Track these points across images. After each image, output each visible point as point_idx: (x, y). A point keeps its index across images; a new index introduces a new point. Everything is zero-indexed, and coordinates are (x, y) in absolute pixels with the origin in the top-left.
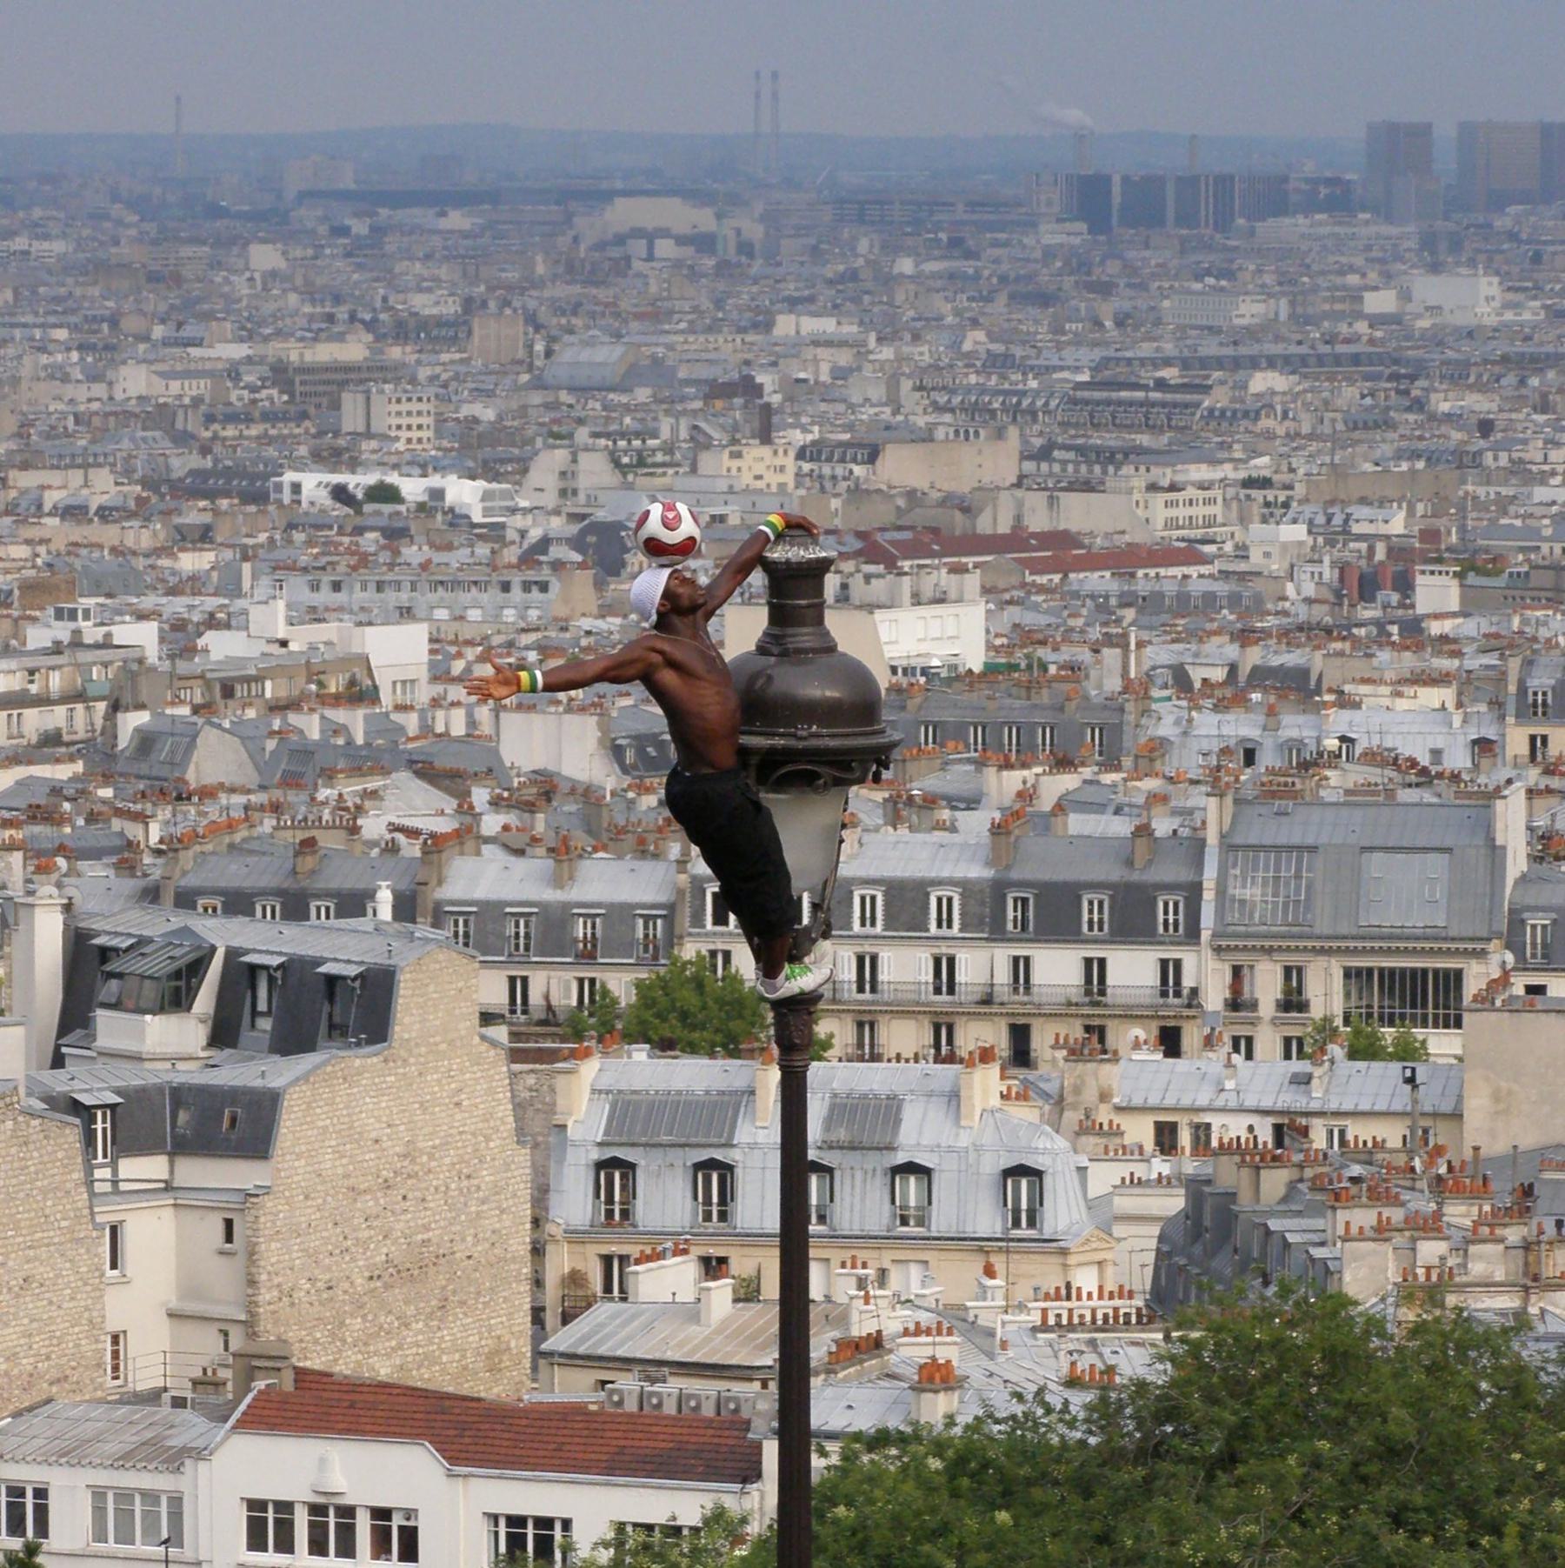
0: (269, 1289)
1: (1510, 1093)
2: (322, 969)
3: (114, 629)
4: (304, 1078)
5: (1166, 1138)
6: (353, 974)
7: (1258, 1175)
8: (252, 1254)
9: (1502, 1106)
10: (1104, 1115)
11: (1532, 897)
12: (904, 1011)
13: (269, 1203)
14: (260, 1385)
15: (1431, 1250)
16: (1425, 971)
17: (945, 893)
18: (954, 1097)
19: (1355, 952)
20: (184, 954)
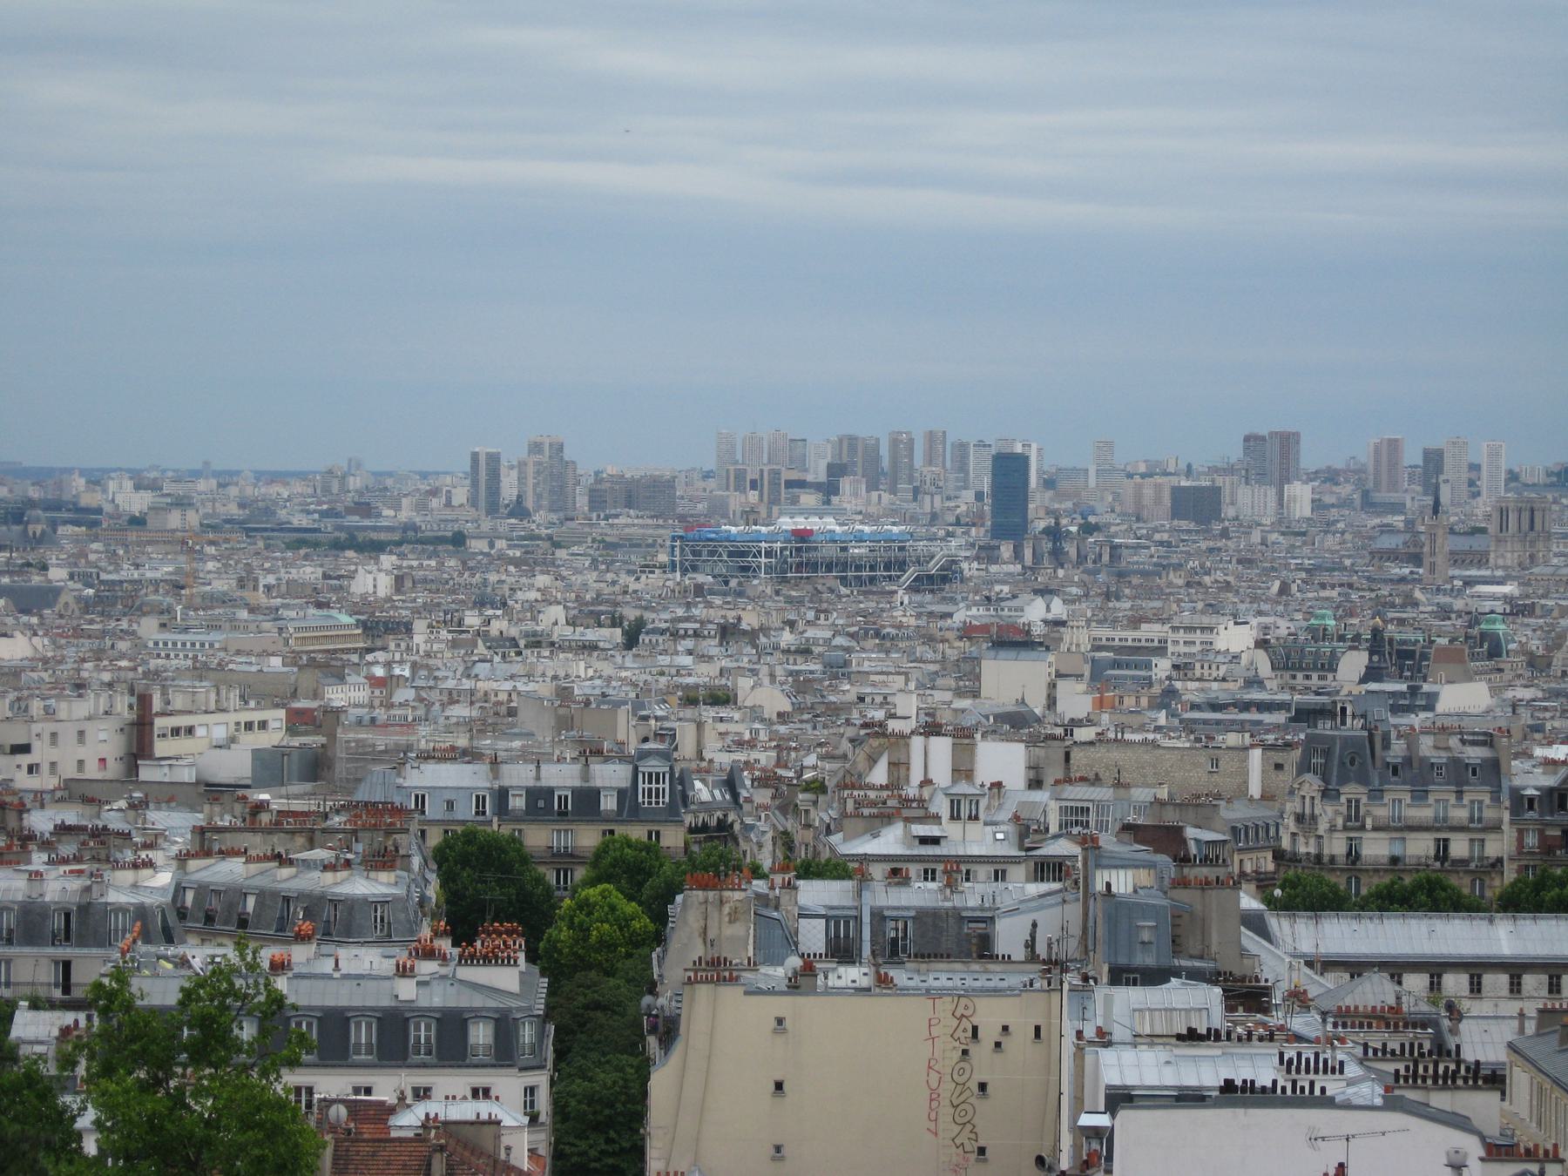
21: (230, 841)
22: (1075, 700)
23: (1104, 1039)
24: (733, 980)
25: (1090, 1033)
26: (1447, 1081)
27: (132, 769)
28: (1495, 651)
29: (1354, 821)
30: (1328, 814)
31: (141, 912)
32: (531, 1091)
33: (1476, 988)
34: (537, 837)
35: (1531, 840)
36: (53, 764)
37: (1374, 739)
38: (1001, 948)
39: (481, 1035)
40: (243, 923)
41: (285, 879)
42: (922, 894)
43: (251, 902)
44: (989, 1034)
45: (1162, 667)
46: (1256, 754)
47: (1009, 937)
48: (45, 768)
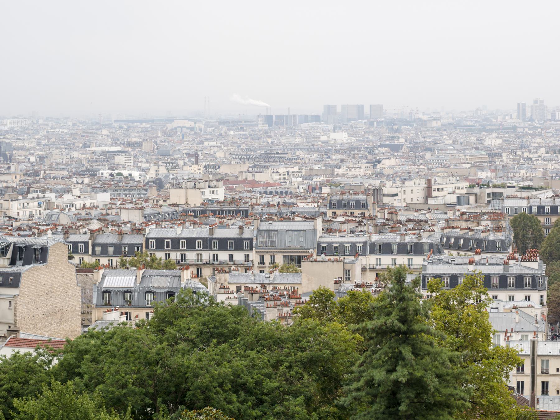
0: (19, 317)
1: (311, 279)
2: (33, 247)
3: (45, 195)
4: (27, 270)
5: (239, 289)
6: (39, 248)
7: (252, 295)
9: (310, 282)
10: (226, 285)
11: (322, 240)
13: (19, 298)
14: (12, 336)
15: (285, 310)
16: (300, 256)
17: (199, 241)
18: (180, 277)
19: (285, 252)
21: (455, 224)
31: (431, 246)
34: (542, 219)
36: (404, 199)
39: (527, 280)
43: (462, 241)
48: (402, 200)
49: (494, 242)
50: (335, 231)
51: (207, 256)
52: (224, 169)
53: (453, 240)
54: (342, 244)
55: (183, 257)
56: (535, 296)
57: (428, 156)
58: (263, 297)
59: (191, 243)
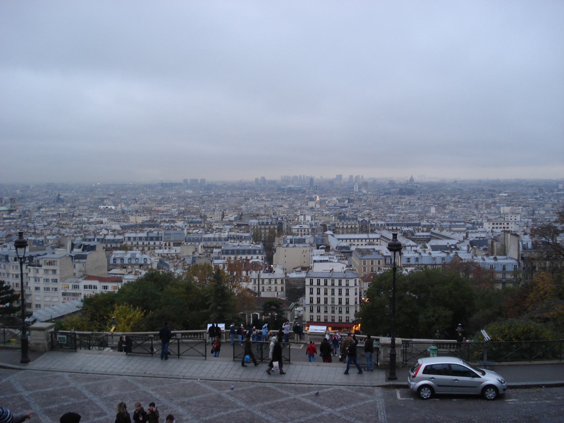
5: (158, 255)
8: (85, 266)
10: (154, 254)
11: (187, 237)
12: (141, 246)
20: (80, 244)
22: (318, 206)
23: (313, 255)
24: (281, 246)
25: (312, 255)
26: (343, 260)
27: (222, 219)
28: (361, 200)
29: (343, 224)
30: (340, 223)
31: (225, 238)
32: (262, 257)
33: (354, 241)
35: (360, 226)
37: (345, 215)
38: (306, 242)
39: (258, 252)
40: (234, 238)
41: (238, 234)
42: (299, 237)
44: (305, 251)
45: (327, 202)
46: (333, 217)
47: (307, 241)
49: (245, 237)
50: (191, 233)
51: (146, 243)
52: (147, 205)
53: (232, 236)
54: (193, 238)
55: (138, 243)
56: (260, 257)
57: (222, 199)
58: (168, 258)
59: (140, 238)
